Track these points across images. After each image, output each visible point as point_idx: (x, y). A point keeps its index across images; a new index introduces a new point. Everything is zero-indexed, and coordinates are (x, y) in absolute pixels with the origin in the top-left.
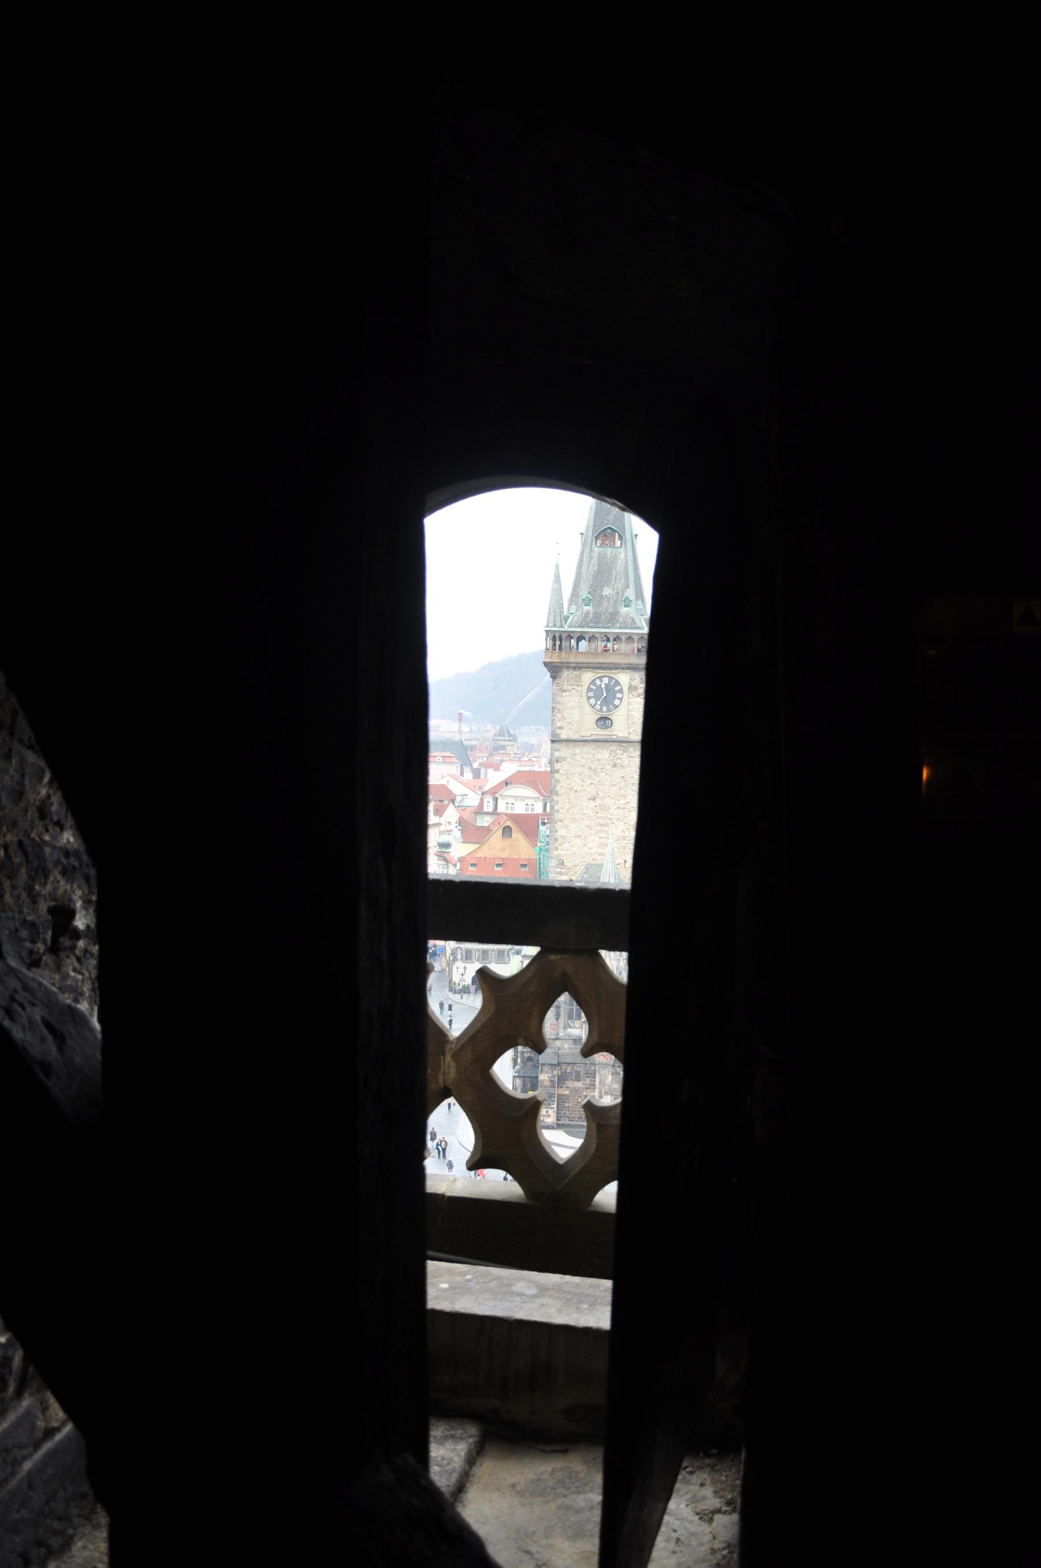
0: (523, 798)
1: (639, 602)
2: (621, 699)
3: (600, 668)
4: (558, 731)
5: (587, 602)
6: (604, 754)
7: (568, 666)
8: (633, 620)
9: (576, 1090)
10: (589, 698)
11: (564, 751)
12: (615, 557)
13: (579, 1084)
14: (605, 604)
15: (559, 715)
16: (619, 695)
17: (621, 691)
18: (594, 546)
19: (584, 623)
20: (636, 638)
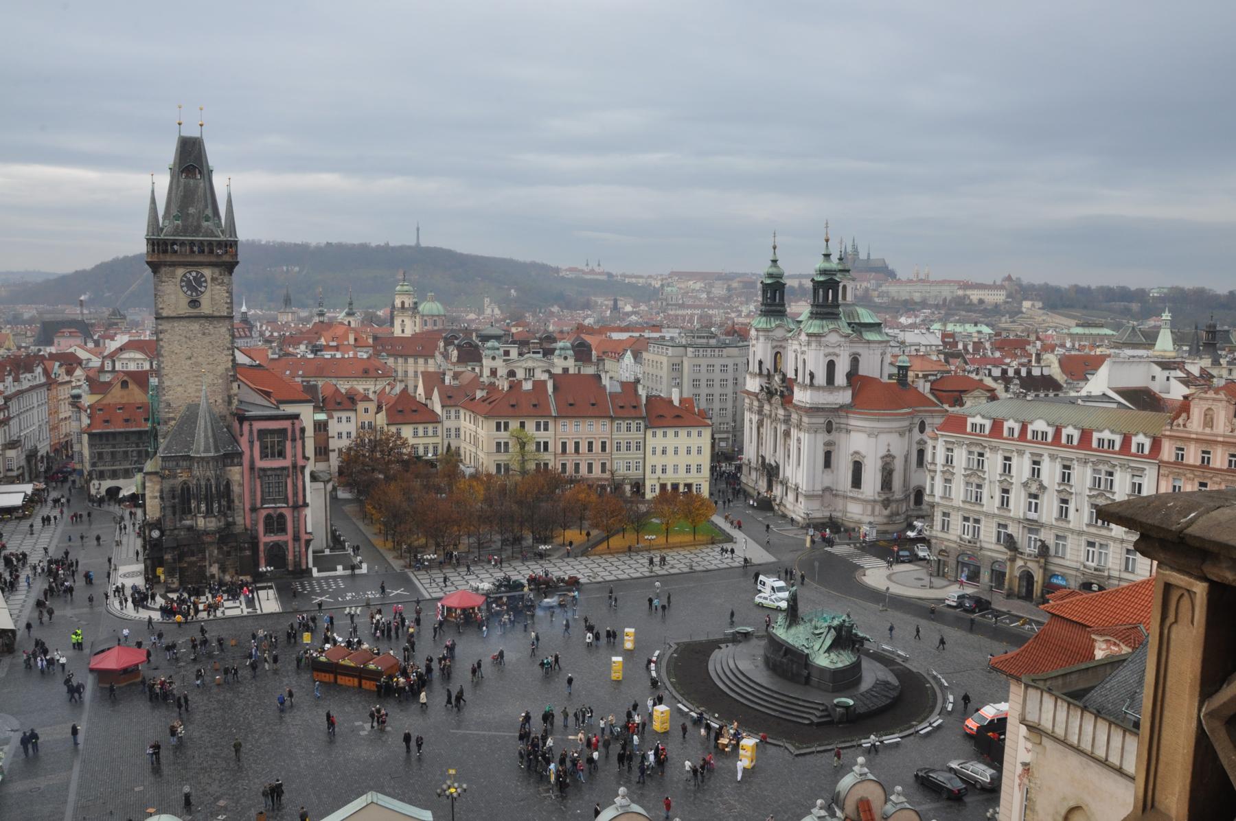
0: (134, 360)
6: (195, 326)
7: (165, 264)
9: (192, 564)
11: (165, 326)
12: (197, 186)
13: (194, 559)
19: (176, 231)
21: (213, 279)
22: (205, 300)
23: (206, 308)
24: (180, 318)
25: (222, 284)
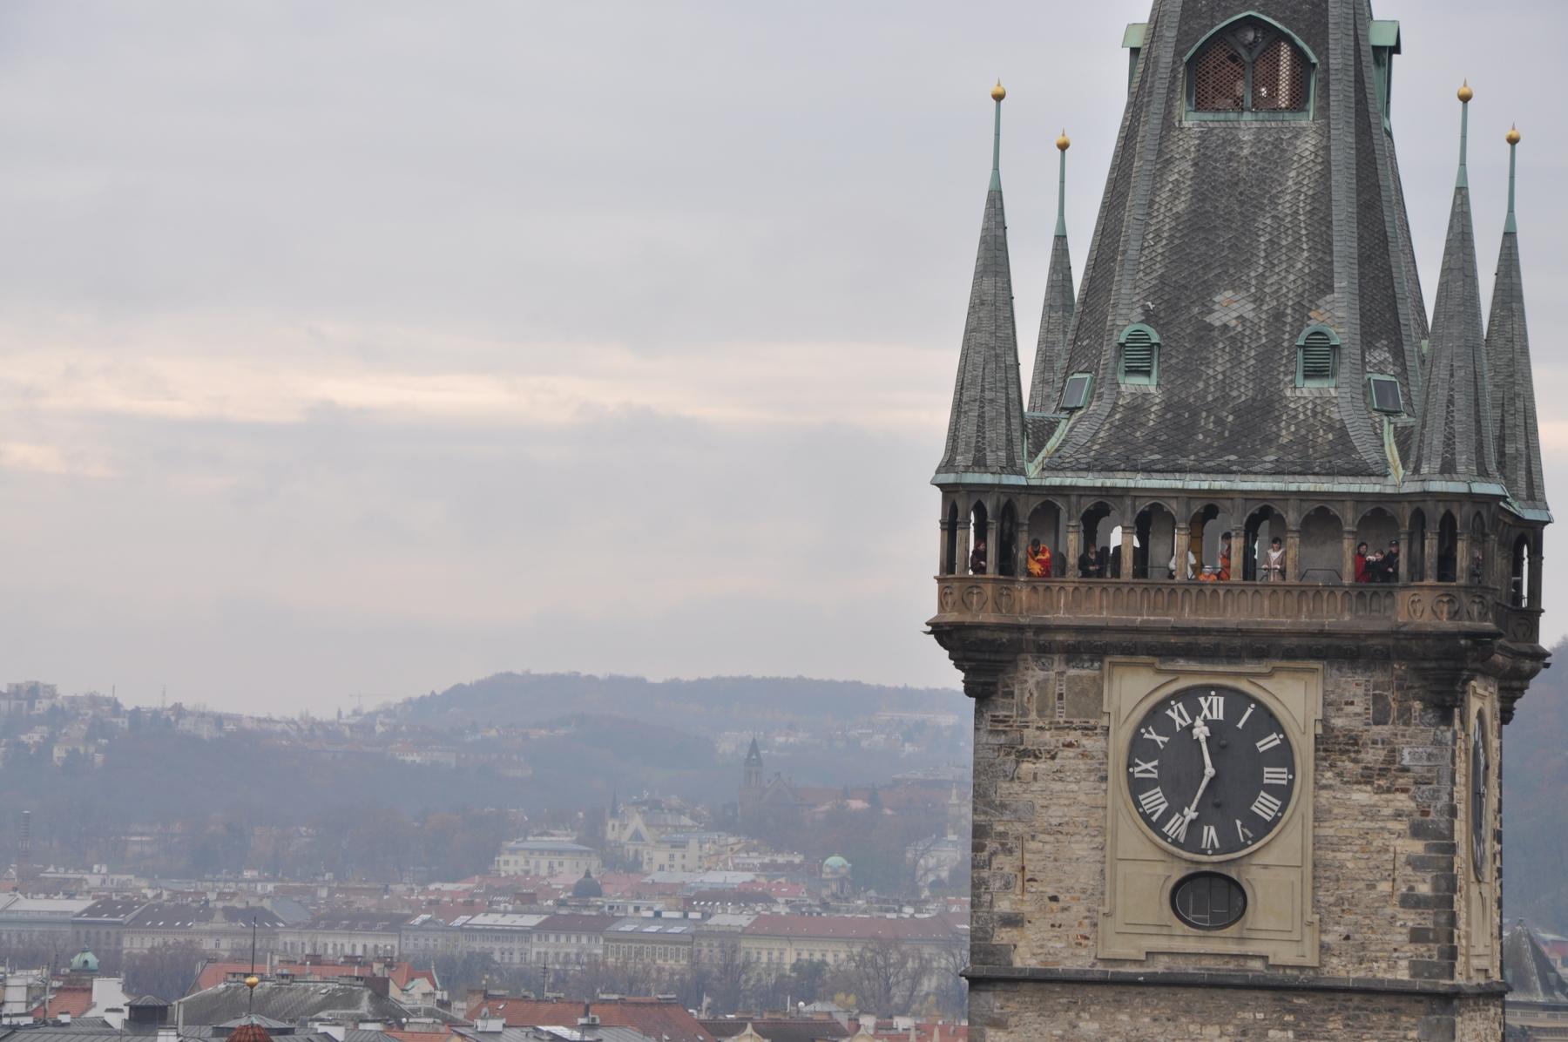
1: (1380, 355)
2: (1283, 793)
3: (1190, 652)
4: (1003, 936)
5: (1137, 357)
7: (1043, 643)
8: (1342, 433)
10: (1137, 787)
12: (1275, 154)
14: (1220, 367)
15: (1005, 863)
16: (1273, 775)
17: (1283, 753)
18: (1181, 106)
19: (1121, 451)
20: (1349, 519)
21: (1329, 744)
22: (1274, 876)
23: (1277, 931)
24: (1115, 984)
25: (1384, 775)
